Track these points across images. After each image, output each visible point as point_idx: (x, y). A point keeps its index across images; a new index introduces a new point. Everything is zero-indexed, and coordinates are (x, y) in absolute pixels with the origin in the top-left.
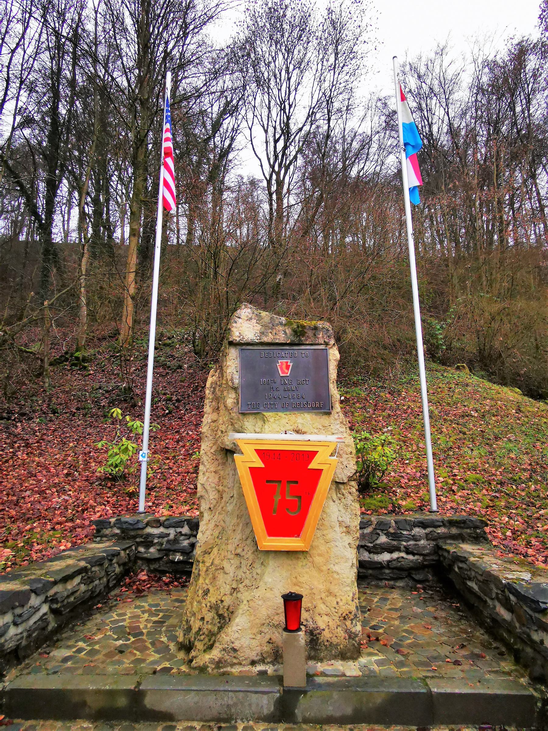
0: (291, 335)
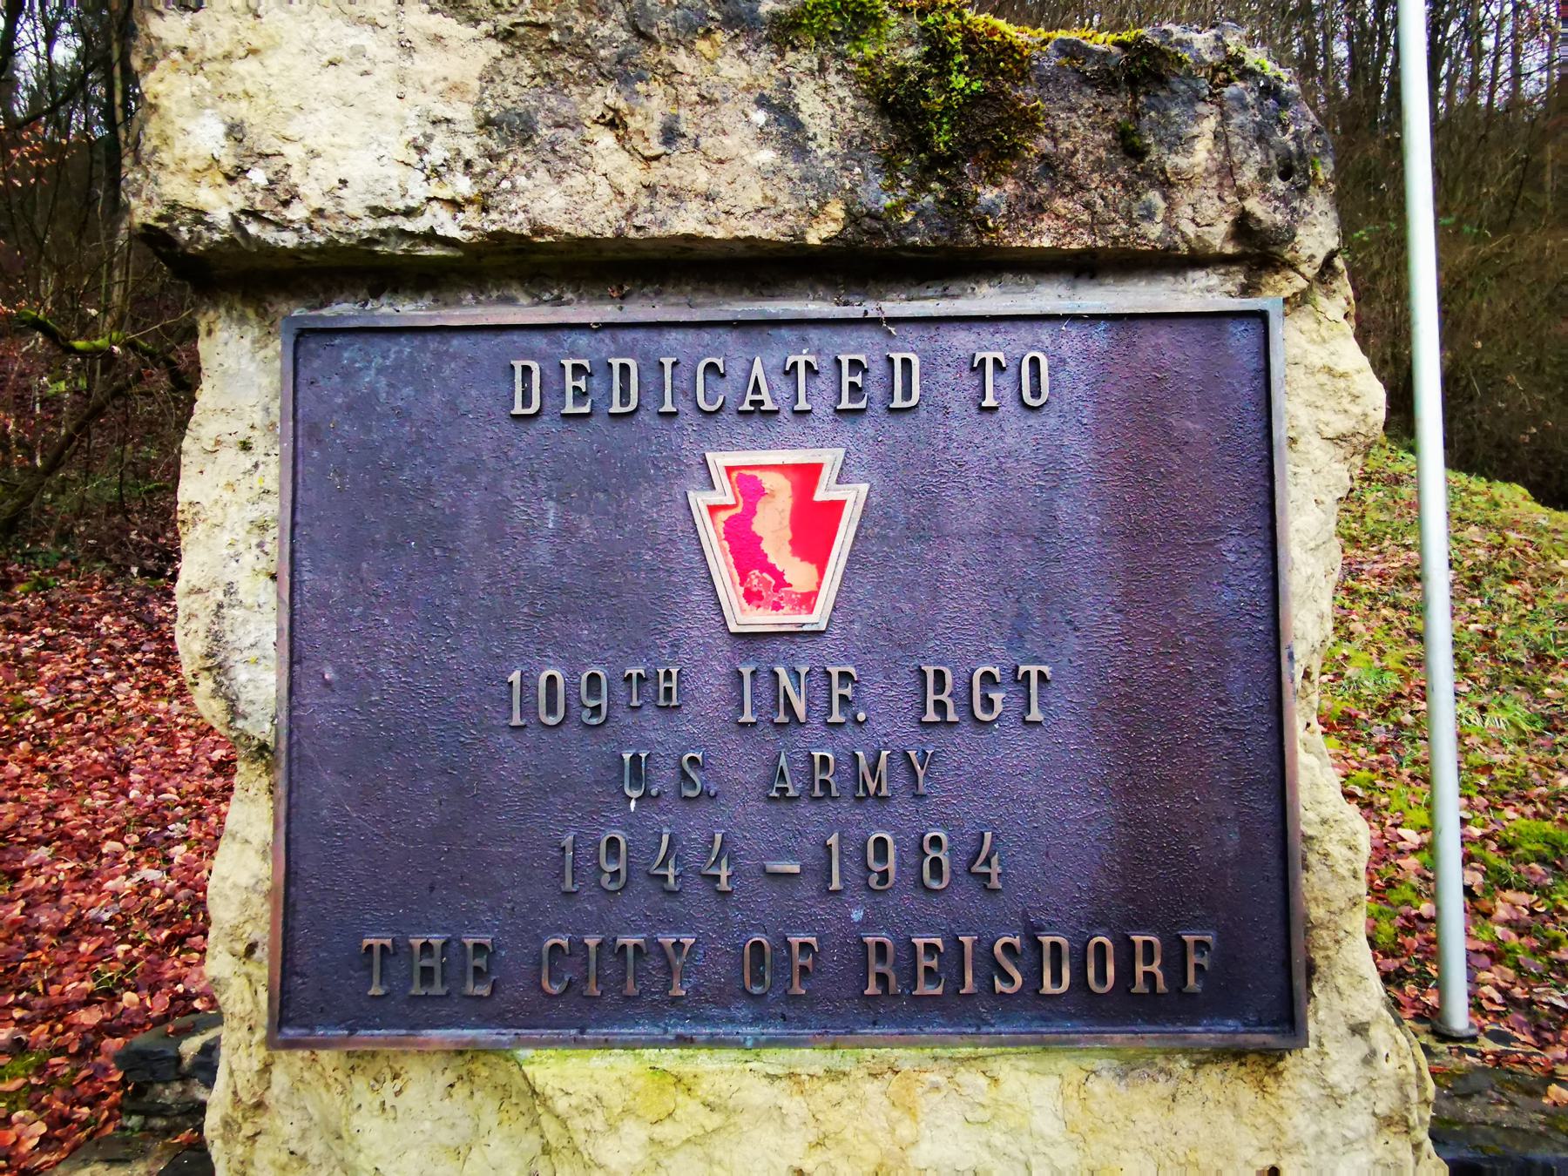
0: (854, 148)
